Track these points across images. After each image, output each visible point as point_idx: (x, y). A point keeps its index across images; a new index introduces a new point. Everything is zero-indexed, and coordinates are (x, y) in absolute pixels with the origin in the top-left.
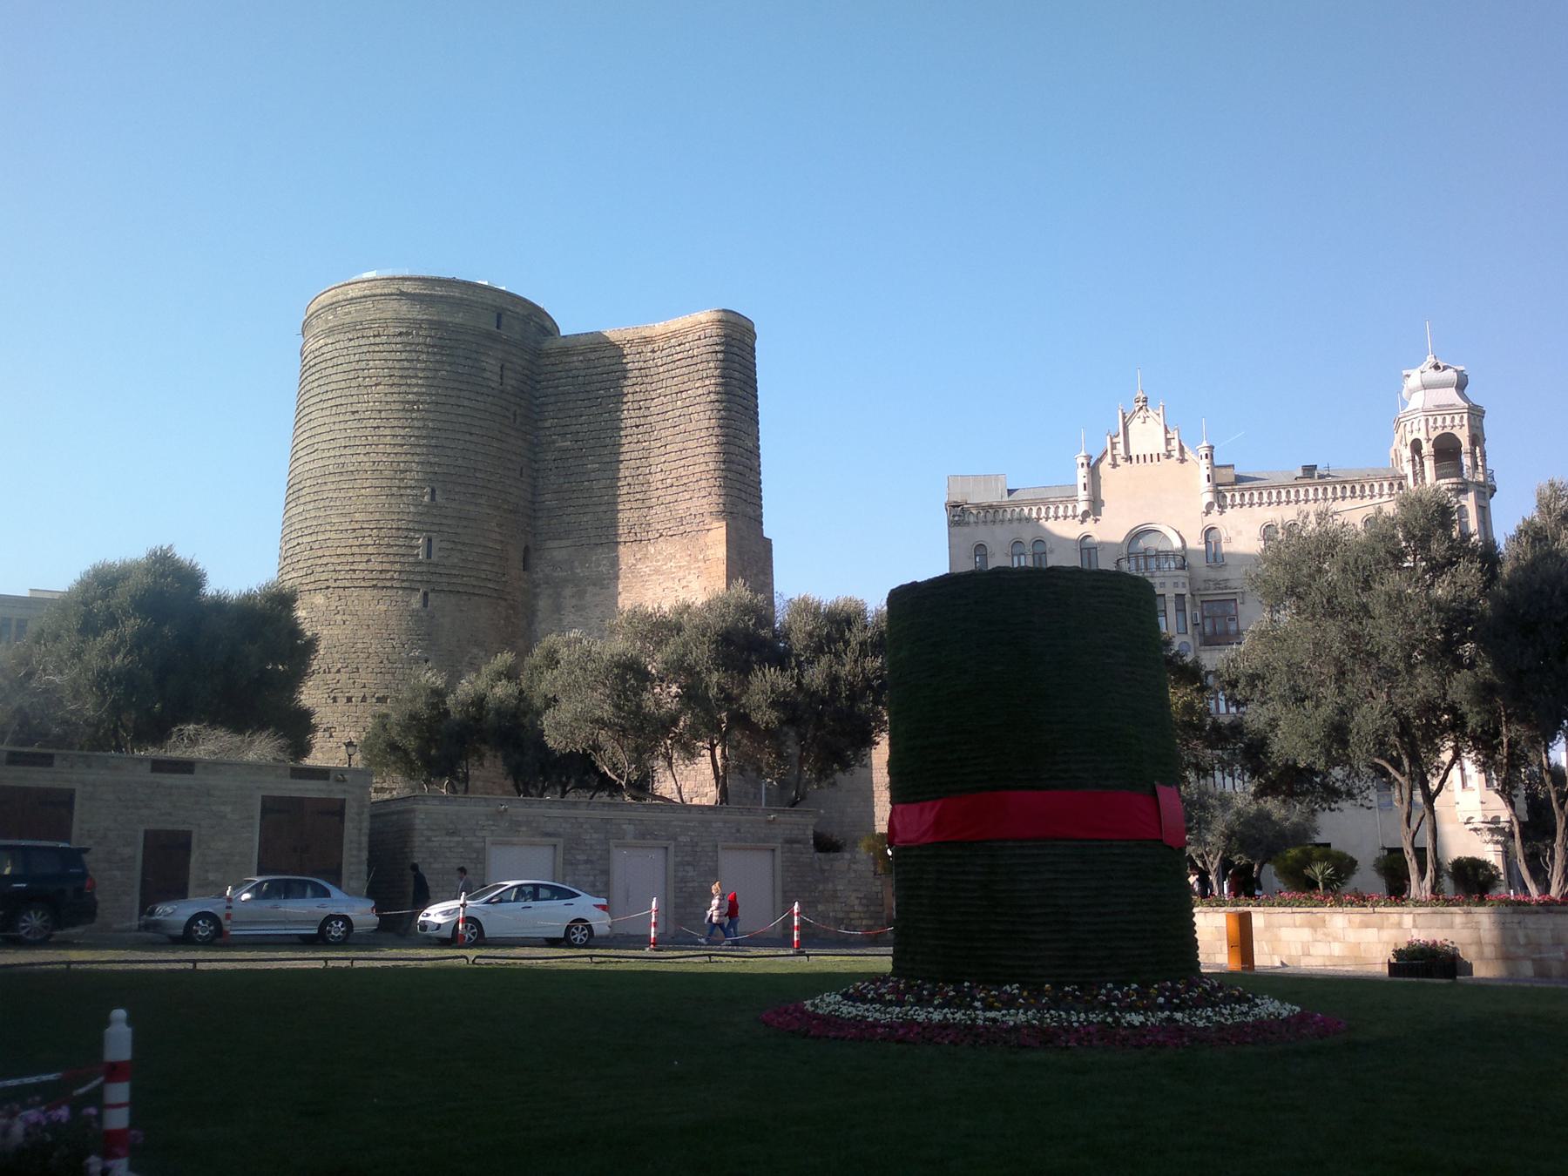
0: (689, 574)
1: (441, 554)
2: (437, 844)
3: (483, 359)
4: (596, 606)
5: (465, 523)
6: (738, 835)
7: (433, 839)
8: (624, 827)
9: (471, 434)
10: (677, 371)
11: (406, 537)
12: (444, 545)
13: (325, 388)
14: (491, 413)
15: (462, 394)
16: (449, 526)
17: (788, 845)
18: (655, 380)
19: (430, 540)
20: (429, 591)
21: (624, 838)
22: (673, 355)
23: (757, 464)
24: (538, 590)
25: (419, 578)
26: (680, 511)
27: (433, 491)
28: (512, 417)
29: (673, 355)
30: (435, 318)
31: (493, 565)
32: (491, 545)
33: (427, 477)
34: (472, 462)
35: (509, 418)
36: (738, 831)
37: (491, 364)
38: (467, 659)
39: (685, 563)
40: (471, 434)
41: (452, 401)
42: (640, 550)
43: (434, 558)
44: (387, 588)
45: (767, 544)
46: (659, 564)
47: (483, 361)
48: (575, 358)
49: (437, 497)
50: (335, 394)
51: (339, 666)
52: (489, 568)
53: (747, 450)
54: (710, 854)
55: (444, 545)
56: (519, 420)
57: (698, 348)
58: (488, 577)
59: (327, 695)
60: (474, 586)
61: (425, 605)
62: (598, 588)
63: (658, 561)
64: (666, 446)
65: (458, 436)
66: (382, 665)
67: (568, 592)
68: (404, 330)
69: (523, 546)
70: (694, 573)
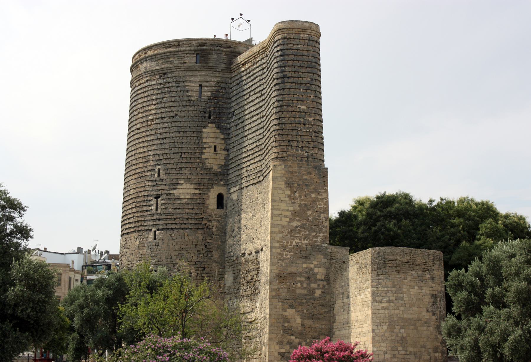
3: (186, 84)
9: (180, 132)
11: (147, 200)
25: (152, 223)
31: (193, 209)
33: (156, 163)
34: (180, 149)
37: (193, 86)
41: (169, 114)
43: (159, 210)
44: (139, 231)
45: (323, 174)
47: (187, 86)
49: (162, 176)
52: (191, 211)
60: (181, 224)
61: (155, 239)
68: (148, 78)
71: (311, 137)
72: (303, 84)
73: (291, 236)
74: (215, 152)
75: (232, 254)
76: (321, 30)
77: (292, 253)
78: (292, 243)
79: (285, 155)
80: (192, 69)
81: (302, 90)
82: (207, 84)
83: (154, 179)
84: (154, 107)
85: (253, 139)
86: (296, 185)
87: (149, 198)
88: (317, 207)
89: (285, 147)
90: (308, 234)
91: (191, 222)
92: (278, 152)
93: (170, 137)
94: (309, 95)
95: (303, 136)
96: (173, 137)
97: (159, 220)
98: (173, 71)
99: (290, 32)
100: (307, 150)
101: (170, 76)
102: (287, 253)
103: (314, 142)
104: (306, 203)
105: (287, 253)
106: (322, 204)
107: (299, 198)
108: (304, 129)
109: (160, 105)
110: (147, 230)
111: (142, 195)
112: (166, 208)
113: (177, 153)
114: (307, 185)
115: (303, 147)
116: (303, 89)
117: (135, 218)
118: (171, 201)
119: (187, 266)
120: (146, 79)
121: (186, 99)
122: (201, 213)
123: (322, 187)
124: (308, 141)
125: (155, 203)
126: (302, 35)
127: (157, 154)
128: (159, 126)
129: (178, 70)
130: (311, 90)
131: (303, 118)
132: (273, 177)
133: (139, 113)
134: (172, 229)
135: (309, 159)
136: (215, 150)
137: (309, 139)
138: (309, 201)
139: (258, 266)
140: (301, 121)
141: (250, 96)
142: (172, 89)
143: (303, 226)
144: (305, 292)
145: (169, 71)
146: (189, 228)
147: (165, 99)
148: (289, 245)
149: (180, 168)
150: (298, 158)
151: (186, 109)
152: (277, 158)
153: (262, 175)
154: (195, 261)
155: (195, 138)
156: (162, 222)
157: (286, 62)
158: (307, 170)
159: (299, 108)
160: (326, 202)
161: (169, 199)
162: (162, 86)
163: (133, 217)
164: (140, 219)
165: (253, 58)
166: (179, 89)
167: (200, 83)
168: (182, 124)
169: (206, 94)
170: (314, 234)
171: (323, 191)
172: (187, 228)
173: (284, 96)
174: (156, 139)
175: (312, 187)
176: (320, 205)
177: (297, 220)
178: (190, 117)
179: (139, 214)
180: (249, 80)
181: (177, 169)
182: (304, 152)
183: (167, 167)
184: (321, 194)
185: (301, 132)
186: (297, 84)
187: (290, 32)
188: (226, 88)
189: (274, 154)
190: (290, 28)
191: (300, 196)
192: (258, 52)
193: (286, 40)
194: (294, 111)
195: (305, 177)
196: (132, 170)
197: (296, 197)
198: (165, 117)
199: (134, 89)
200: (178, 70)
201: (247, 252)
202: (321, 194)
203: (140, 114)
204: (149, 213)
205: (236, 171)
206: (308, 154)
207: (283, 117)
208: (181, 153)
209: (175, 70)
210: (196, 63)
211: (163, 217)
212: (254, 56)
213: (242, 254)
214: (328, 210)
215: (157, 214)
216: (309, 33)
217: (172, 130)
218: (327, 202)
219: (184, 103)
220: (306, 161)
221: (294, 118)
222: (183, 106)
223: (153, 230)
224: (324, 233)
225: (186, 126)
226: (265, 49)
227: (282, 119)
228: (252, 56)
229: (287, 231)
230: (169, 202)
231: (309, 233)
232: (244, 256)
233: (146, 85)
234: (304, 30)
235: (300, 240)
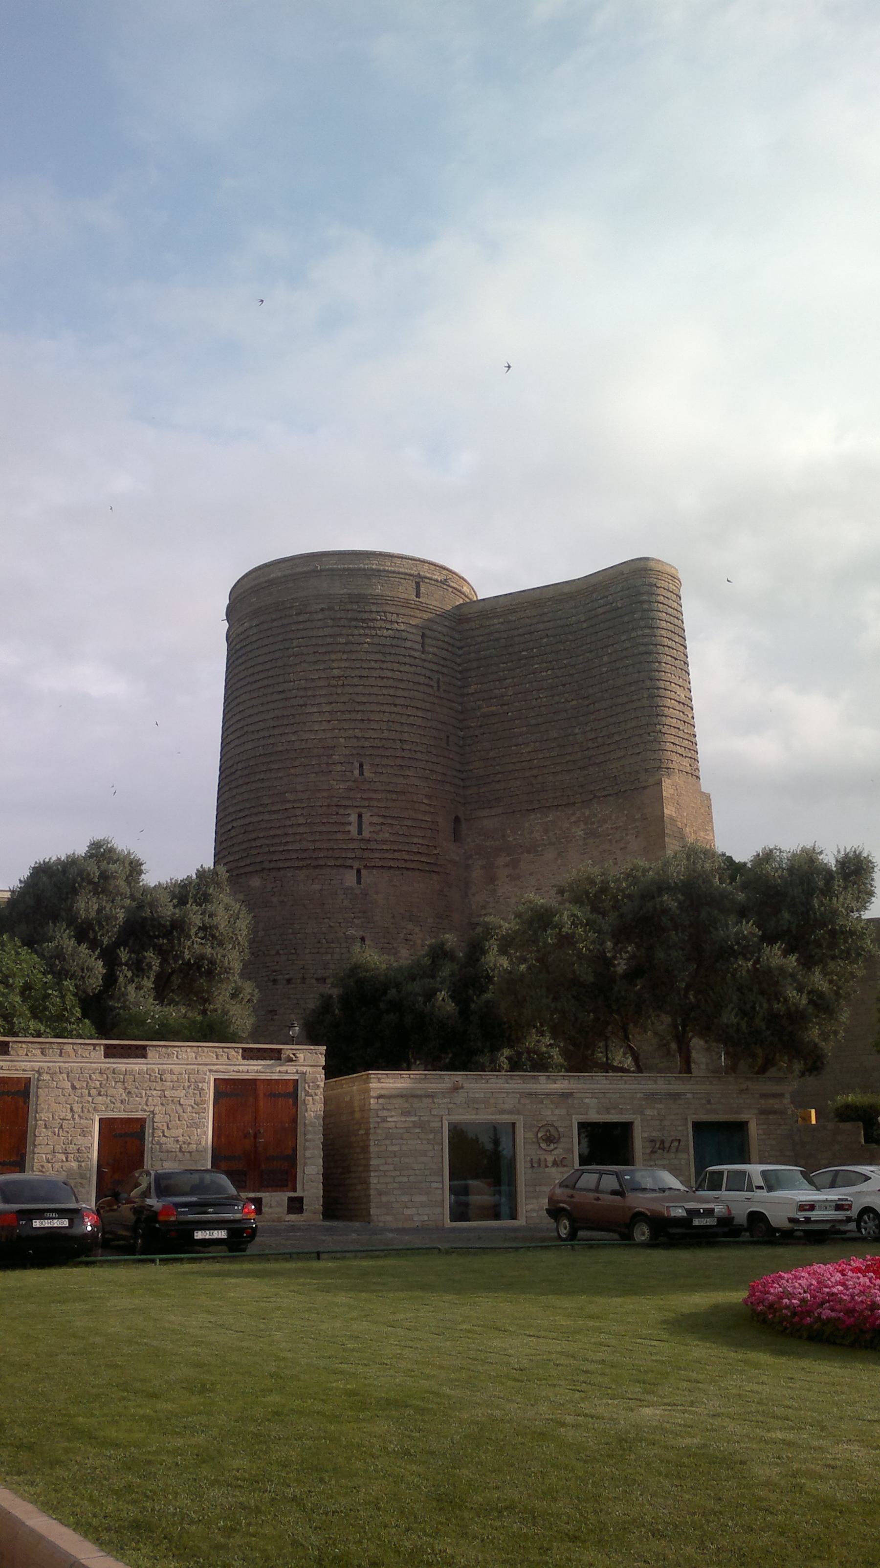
0: (627, 835)
2: (392, 1125)
4: (531, 874)
5: (394, 796)
6: (708, 1106)
7: (389, 1119)
8: (587, 1101)
9: (395, 705)
10: (602, 625)
12: (375, 820)
13: (251, 671)
15: (384, 666)
16: (378, 800)
17: (763, 1117)
18: (579, 637)
19: (360, 816)
21: (586, 1114)
22: (596, 609)
23: (690, 716)
24: (470, 862)
26: (614, 770)
27: (361, 766)
28: (435, 685)
29: (596, 609)
32: (420, 817)
33: (354, 752)
35: (432, 687)
36: (709, 1102)
38: (402, 935)
39: (621, 824)
40: (395, 705)
41: (376, 673)
42: (573, 814)
43: (366, 834)
46: (595, 826)
48: (496, 621)
50: (262, 676)
51: (278, 947)
52: (421, 841)
53: (679, 702)
54: (680, 1128)
55: (375, 820)
57: (622, 599)
58: (420, 851)
59: (266, 979)
61: (359, 882)
62: (532, 855)
63: (593, 823)
64: (594, 703)
65: (383, 708)
66: (319, 945)
67: (502, 860)
70: (632, 834)
87: (342, 811)
91: (422, 860)
93: (379, 712)
111: (325, 804)
112: (377, 833)
118: (390, 821)
127: (355, 737)
129: (389, 602)
134: (391, 867)
136: (448, 744)
161: (384, 816)
169: (431, 650)
183: (377, 761)
198: (367, 677)
200: (389, 602)
204: (340, 836)
219: (402, 659)
230: (381, 820)
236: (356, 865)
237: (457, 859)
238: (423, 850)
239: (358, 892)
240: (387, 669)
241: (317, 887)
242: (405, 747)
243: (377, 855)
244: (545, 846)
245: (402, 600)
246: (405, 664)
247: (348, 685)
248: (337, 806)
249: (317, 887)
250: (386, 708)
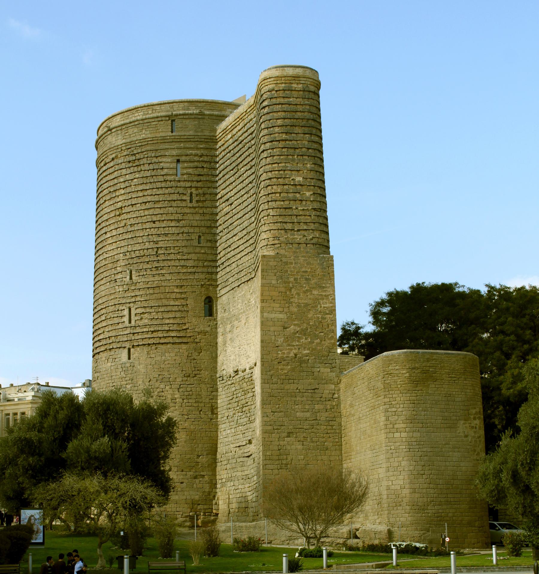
1: (137, 318)
5: (151, 291)
9: (154, 222)
14: (169, 201)
20: (131, 347)
30: (128, 140)
31: (174, 318)
32: (172, 303)
40: (154, 222)
41: (140, 200)
44: (110, 349)
49: (134, 278)
52: (171, 321)
55: (140, 311)
56: (195, 199)
60: (160, 338)
61: (129, 358)
67: (228, 327)
68: (114, 156)
69: (203, 298)
71: (309, 217)
72: (297, 148)
73: (289, 345)
74: (199, 245)
75: (224, 372)
76: (321, 78)
77: (289, 367)
78: (289, 353)
79: (276, 242)
80: (168, 141)
81: (296, 157)
82: (188, 158)
83: (126, 283)
84: (122, 192)
85: (244, 224)
86: (292, 280)
88: (321, 307)
89: (276, 231)
90: (310, 342)
91: (173, 335)
92: (268, 238)
93: (143, 229)
94: (306, 162)
95: (300, 215)
96: (146, 229)
97: (134, 334)
98: (143, 144)
99: (278, 82)
100: (306, 233)
101: (140, 151)
102: (282, 367)
103: (314, 223)
104: (306, 301)
105: (282, 367)
106: (326, 303)
107: (296, 296)
108: (301, 207)
109: (129, 190)
110: (120, 348)
112: (141, 319)
113: (152, 248)
114: (306, 279)
115: (298, 230)
116: (298, 155)
117: (105, 333)
119: (169, 391)
120: (111, 157)
121: (161, 179)
122: (185, 324)
123: (326, 280)
124: (307, 223)
125: (128, 311)
126: (295, 86)
128: (129, 216)
129: (150, 142)
130: (309, 156)
131: (299, 193)
132: (263, 271)
133: (105, 201)
134: (149, 344)
135: (308, 245)
137: (307, 219)
138: (310, 299)
139: (252, 386)
140: (296, 197)
141: (238, 170)
142: (143, 168)
143: (304, 332)
144: (308, 415)
145: (138, 145)
146: (170, 343)
147: (135, 180)
148: (285, 356)
149: (156, 267)
150: (294, 245)
151: (160, 192)
152: (267, 245)
153: (254, 270)
154: (179, 383)
155: (174, 229)
156: (136, 337)
157: (275, 121)
158: (307, 260)
159: (292, 180)
160: (332, 299)
162: (131, 164)
163: (104, 332)
164: (110, 334)
165: (240, 121)
166: (151, 167)
167: (178, 158)
168: (158, 211)
170: (318, 341)
171: (328, 285)
172: (167, 343)
173: (273, 165)
174: (126, 232)
175: (313, 282)
176: (323, 304)
177: (295, 325)
178: (166, 202)
179: (110, 328)
180: (237, 149)
181: (152, 269)
182: (302, 237)
184: (325, 289)
185: (297, 210)
186: (289, 149)
187: (278, 82)
188: (211, 162)
189: (263, 241)
190: (278, 77)
191: (298, 294)
192: (246, 112)
193: (274, 92)
194: (287, 184)
195: (303, 270)
196: (100, 274)
197: (292, 295)
198: (136, 204)
199: (99, 171)
200: (150, 142)
201: (241, 368)
202: (325, 289)
203: (107, 202)
204: (121, 326)
205: (226, 267)
206: (307, 239)
207: (272, 193)
208: (158, 248)
209: (146, 143)
210: (172, 132)
211: (138, 330)
212: (241, 118)
213: (236, 372)
214: (335, 310)
215: (131, 327)
216: (304, 82)
217: (144, 219)
218: (334, 299)
219: (159, 185)
220: (303, 248)
221: (287, 193)
222: (157, 188)
223: (127, 348)
224: (329, 339)
225: (162, 214)
226: (252, 107)
227: (272, 195)
228: (238, 118)
229: (282, 340)
230: (143, 310)
231: (311, 340)
232: (237, 374)
233: (112, 164)
234: (296, 78)
235: (299, 349)
236: (128, 345)
237: (208, 329)
238: (175, 327)
239: (128, 365)
240: (148, 195)
241: (109, 364)
242: (160, 252)
243: (140, 337)
244: (242, 313)
245: (160, 138)
246: (162, 188)
247: (125, 213)
248: (119, 304)
249: (109, 364)
250: (148, 225)
